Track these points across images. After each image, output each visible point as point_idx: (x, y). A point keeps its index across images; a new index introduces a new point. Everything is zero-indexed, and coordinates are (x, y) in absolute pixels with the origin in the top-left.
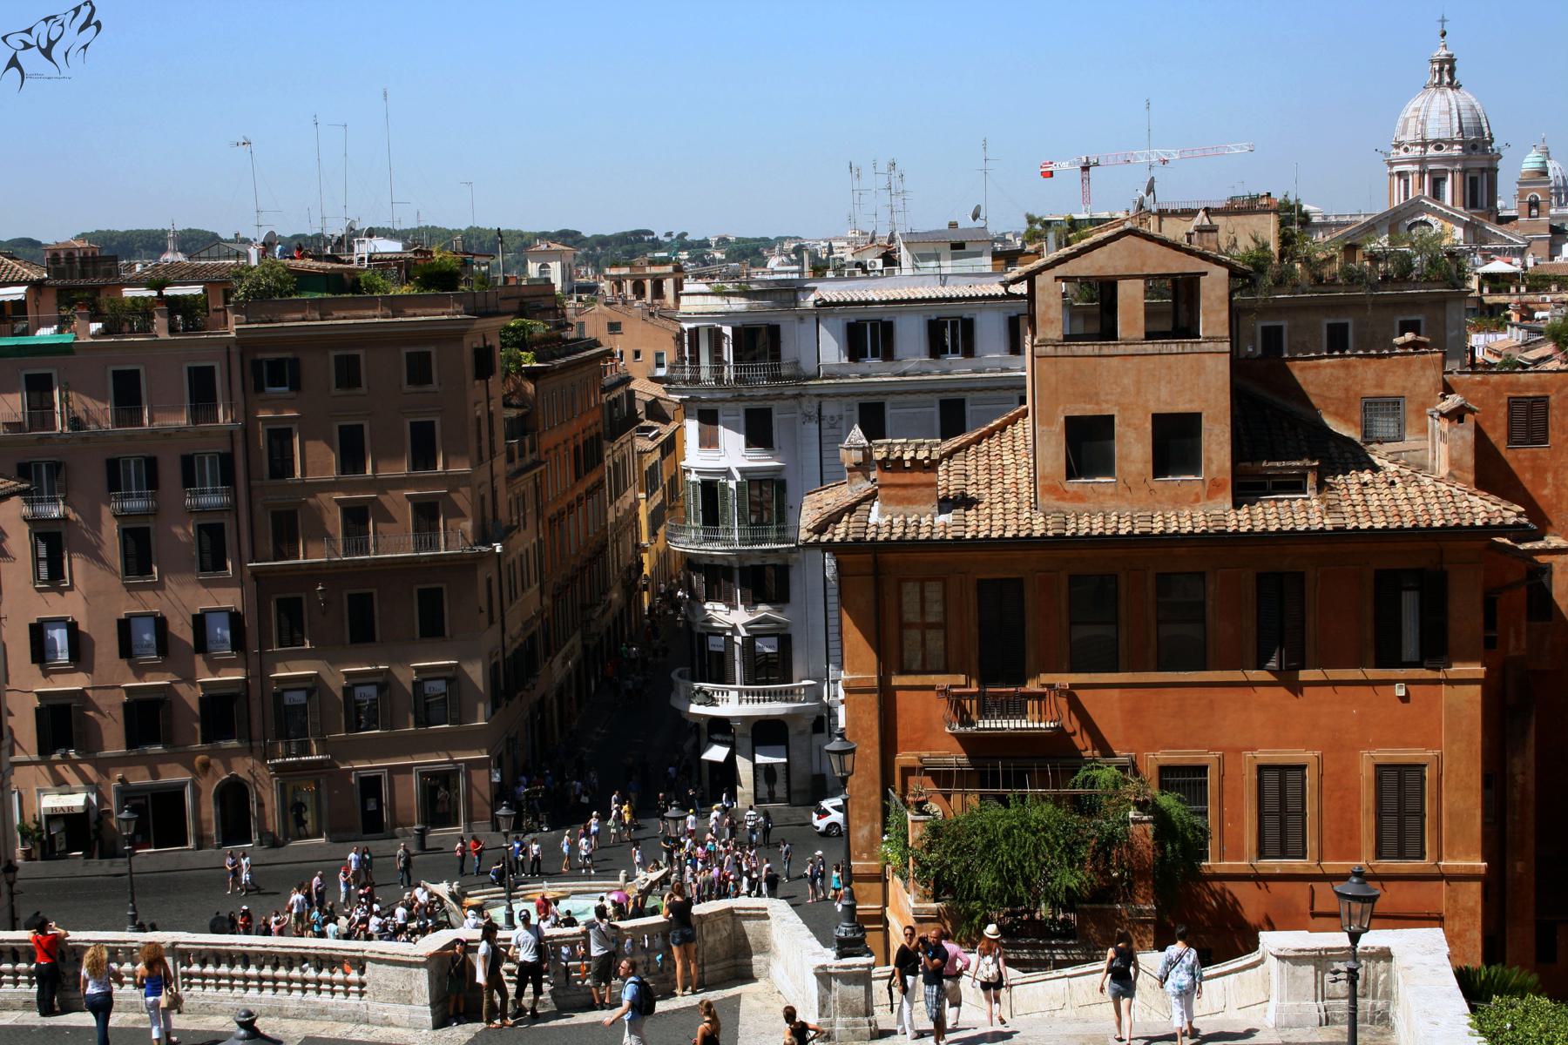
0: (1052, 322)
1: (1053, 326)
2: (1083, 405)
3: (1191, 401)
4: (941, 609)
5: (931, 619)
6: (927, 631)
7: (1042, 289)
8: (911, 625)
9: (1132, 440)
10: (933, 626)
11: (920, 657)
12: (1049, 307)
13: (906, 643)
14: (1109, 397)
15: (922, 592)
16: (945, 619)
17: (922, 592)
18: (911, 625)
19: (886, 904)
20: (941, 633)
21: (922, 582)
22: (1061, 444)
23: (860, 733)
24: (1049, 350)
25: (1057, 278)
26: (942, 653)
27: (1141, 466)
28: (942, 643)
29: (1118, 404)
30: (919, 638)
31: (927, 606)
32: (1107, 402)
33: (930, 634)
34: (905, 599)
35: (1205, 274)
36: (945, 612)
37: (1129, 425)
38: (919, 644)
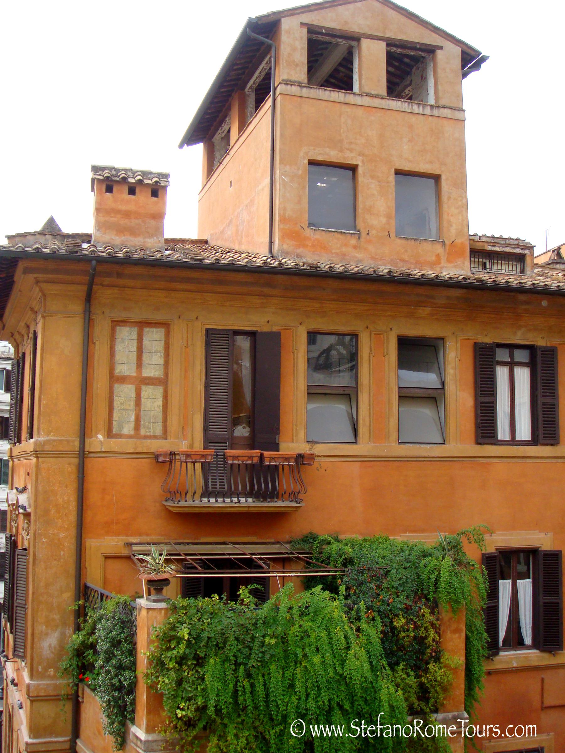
0: (297, 65)
1: (298, 69)
2: (327, 150)
3: (431, 162)
4: (161, 361)
5: (148, 372)
6: (143, 387)
7: (288, 32)
8: (123, 379)
9: (375, 193)
10: (149, 381)
11: (133, 418)
12: (294, 49)
13: (117, 402)
14: (353, 146)
15: (140, 340)
16: (166, 374)
17: (140, 340)
18: (123, 379)
19: (76, 733)
20: (159, 391)
21: (142, 325)
22: (304, 187)
23: (53, 511)
24: (295, 90)
25: (302, 24)
26: (160, 415)
27: (384, 220)
28: (160, 403)
29: (361, 154)
30: (133, 395)
31: (145, 357)
32: (351, 150)
33: (147, 391)
34: (119, 347)
35: (441, 48)
36: (166, 365)
37: (373, 177)
38: (132, 404)
